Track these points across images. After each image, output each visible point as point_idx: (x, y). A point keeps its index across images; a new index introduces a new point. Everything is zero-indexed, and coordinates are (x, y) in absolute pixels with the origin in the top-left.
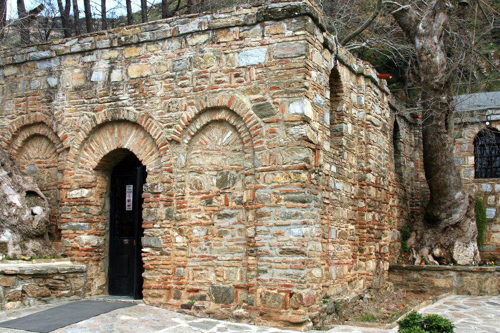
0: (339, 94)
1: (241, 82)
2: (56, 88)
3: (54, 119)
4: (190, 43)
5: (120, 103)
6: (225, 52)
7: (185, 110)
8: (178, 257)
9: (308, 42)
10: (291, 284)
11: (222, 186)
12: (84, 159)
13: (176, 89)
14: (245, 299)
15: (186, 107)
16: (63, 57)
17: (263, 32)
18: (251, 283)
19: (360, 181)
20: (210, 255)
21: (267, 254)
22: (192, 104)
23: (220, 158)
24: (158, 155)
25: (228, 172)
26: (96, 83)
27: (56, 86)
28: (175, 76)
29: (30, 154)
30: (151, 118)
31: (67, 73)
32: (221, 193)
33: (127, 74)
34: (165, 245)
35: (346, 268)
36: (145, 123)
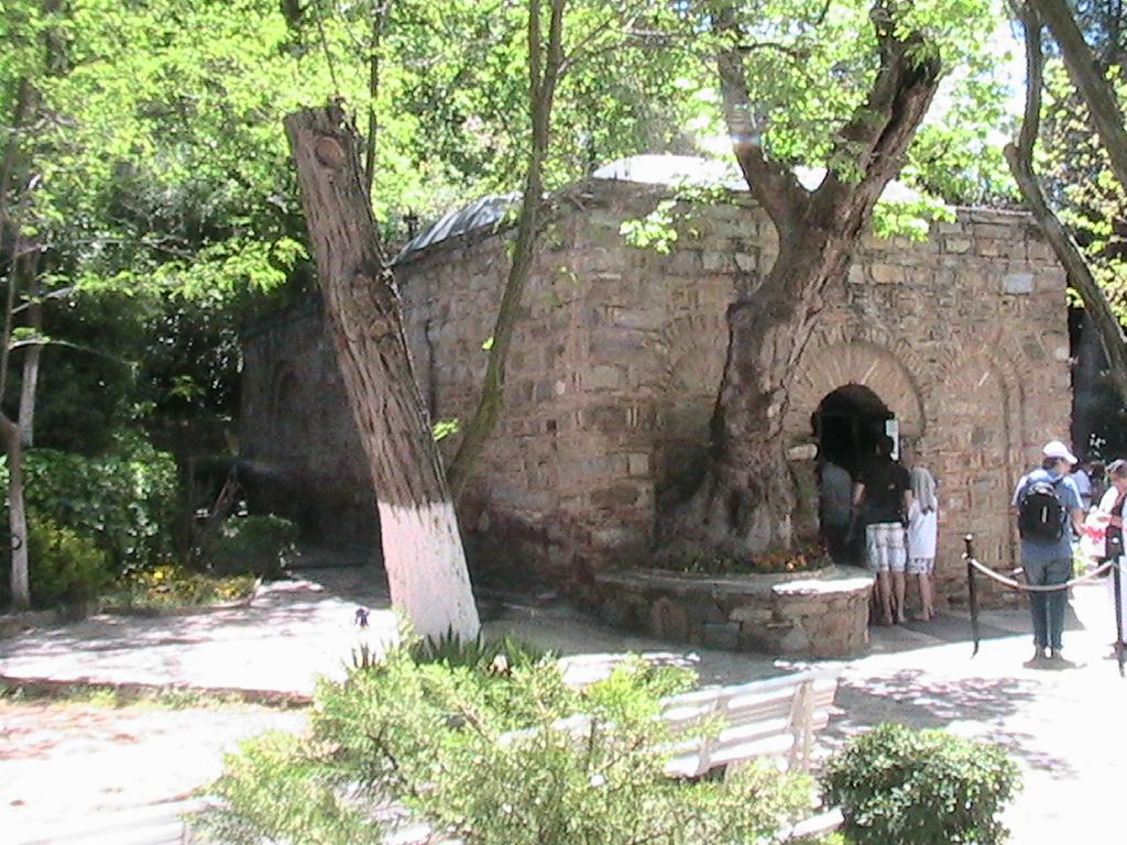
4: (949, 247)
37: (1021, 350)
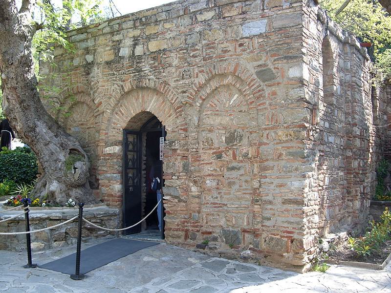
0: (329, 60)
1: (244, 51)
2: (92, 64)
3: (91, 89)
4: (199, 19)
5: (142, 74)
6: (230, 25)
7: (197, 77)
8: (193, 205)
9: (305, 12)
10: (292, 230)
11: (231, 142)
12: (115, 121)
13: (189, 60)
14: (252, 241)
15: (197, 74)
16: (97, 37)
17: (263, 6)
18: (257, 228)
19: (347, 133)
20: (221, 202)
21: (270, 203)
22: (202, 71)
23: (228, 119)
24: (175, 116)
25: (235, 130)
26: (123, 58)
27: (92, 62)
28: (187, 49)
29: (75, 118)
30: (169, 85)
31: (100, 50)
32: (230, 149)
33: (148, 48)
34: (182, 194)
35: (337, 208)
36: (163, 90)
37: (255, 76)
